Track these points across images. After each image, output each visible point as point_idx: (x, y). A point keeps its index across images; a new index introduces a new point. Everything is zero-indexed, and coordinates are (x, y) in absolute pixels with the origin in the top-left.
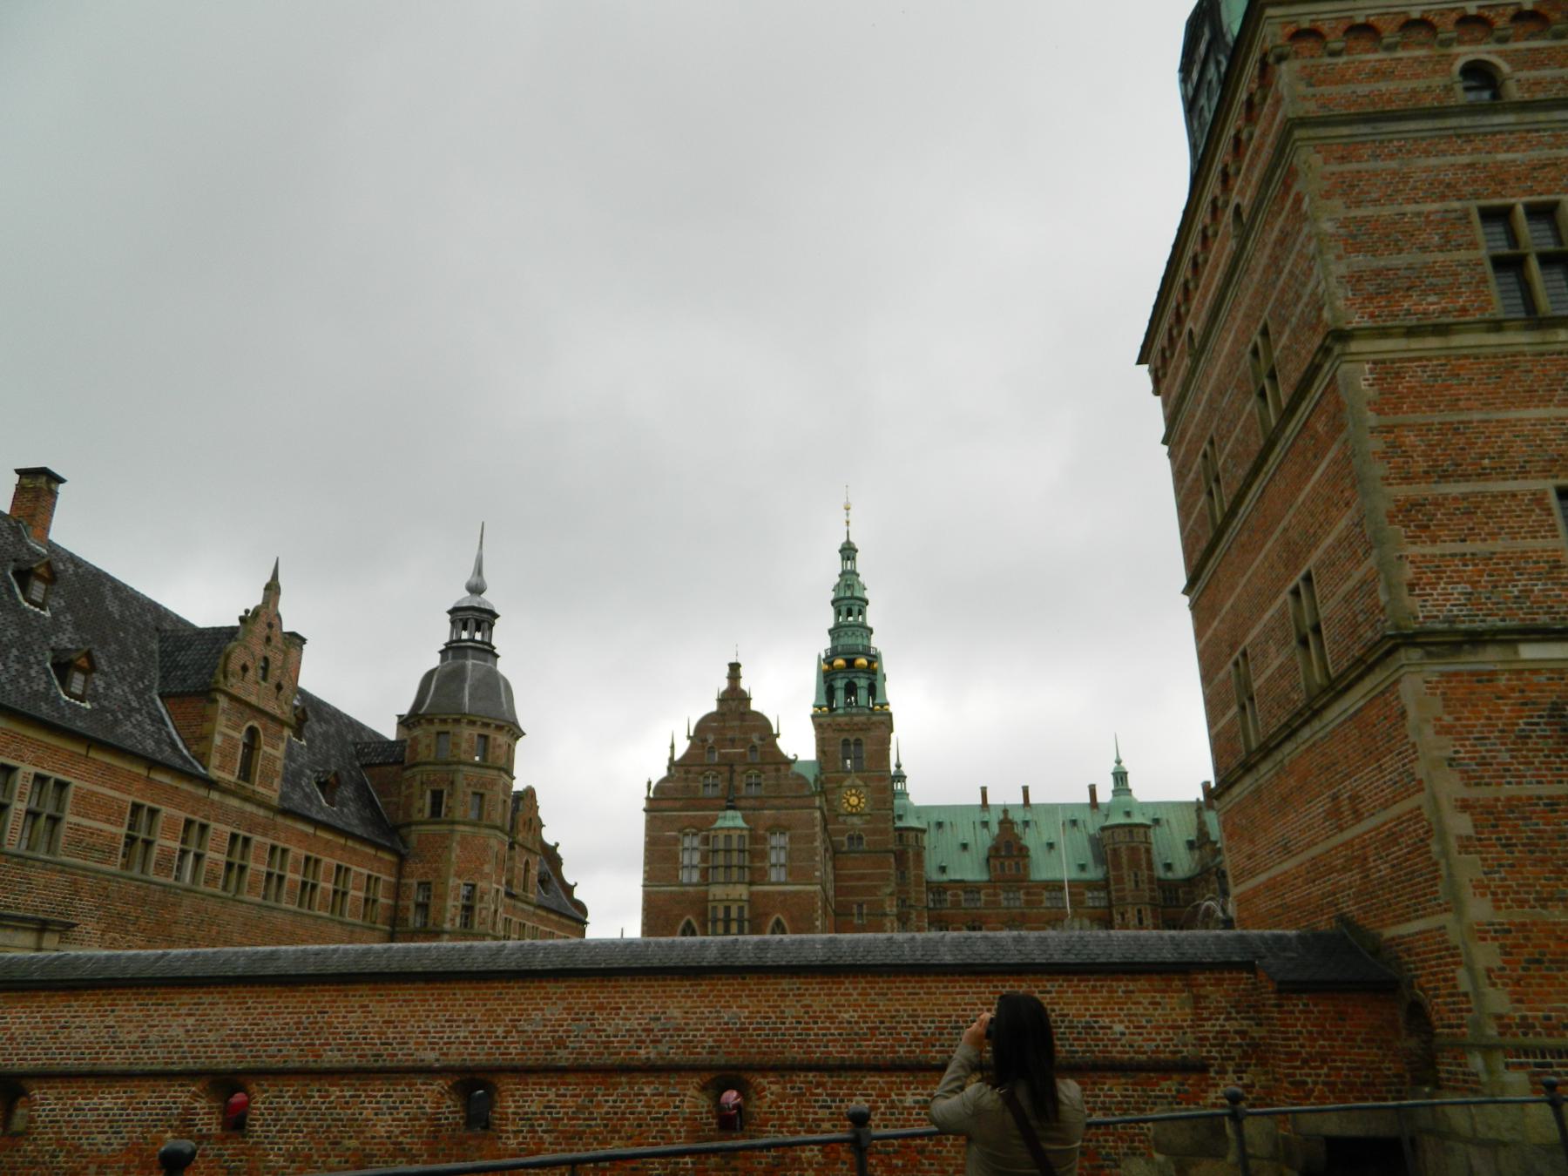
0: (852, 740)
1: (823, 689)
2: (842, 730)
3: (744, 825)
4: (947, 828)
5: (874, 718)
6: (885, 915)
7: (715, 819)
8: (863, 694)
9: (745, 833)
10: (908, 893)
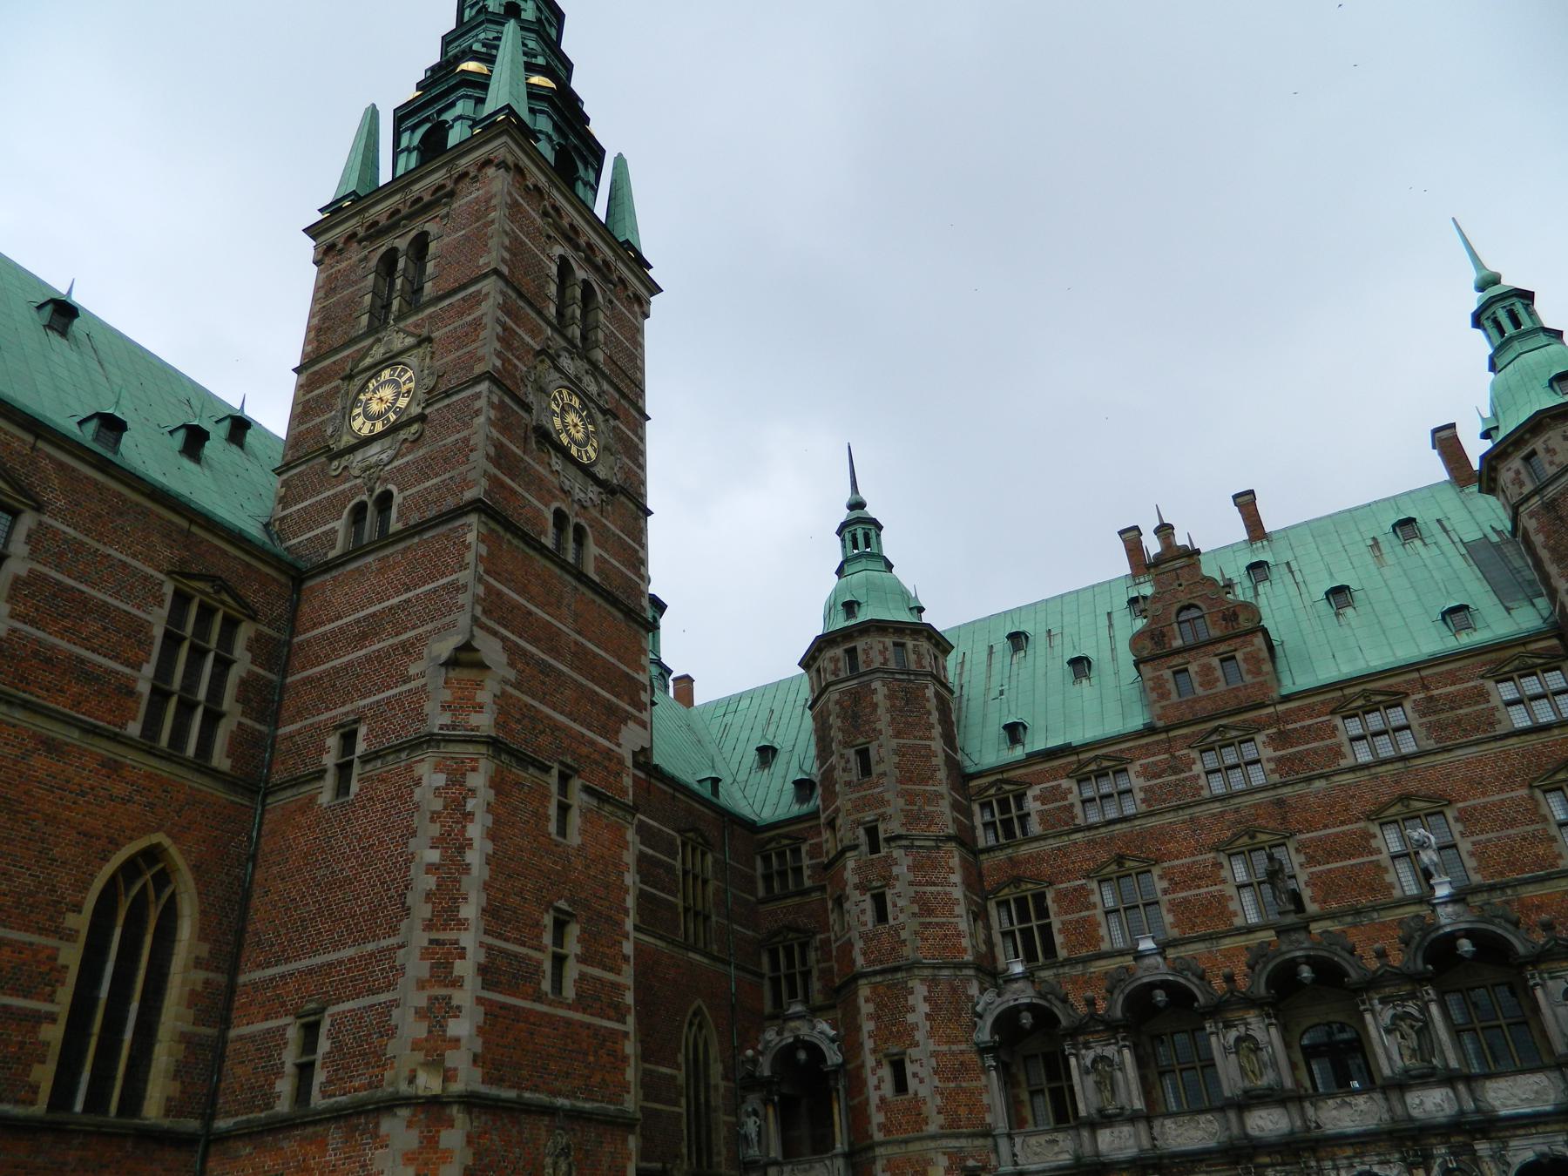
4: (1038, 645)
10: (883, 802)
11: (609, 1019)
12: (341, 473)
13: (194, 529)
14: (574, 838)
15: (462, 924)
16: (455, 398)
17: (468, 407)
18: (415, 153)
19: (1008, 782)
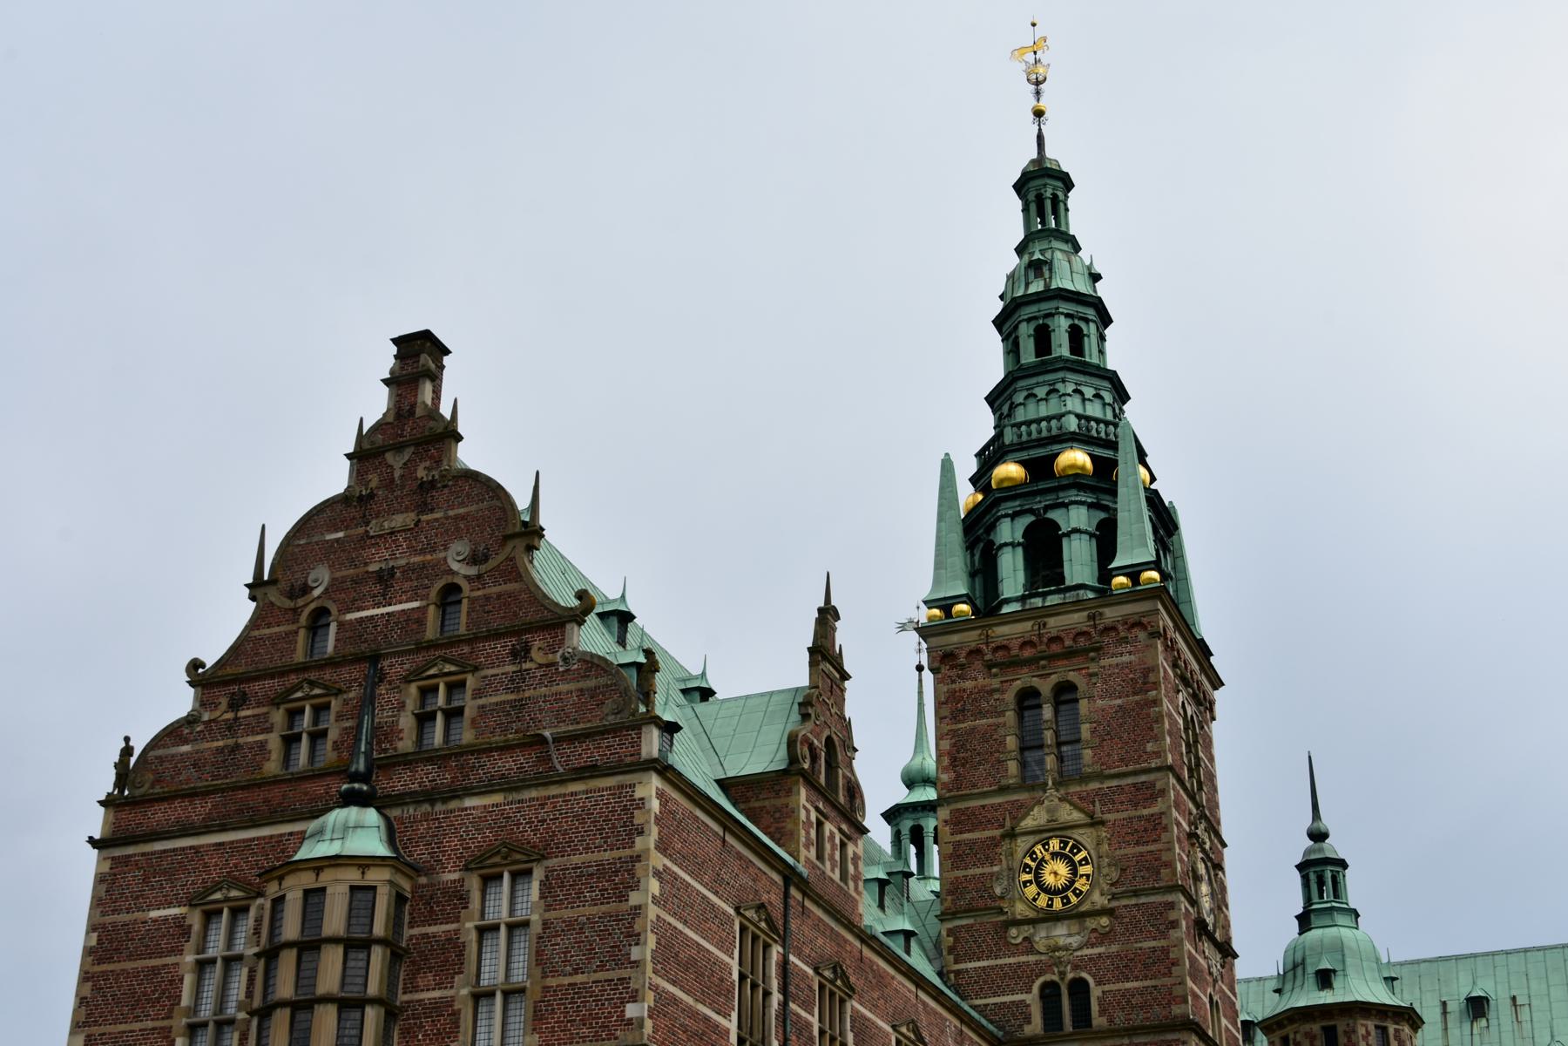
0: (1045, 687)
1: (958, 560)
2: (1016, 664)
3: (382, 850)
4: (1500, 1010)
5: (1111, 614)
7: (302, 837)
8: (1079, 562)
9: (376, 876)
12: (1021, 943)
13: (965, 1029)
16: (1143, 900)
17: (1161, 914)
18: (1020, 551)
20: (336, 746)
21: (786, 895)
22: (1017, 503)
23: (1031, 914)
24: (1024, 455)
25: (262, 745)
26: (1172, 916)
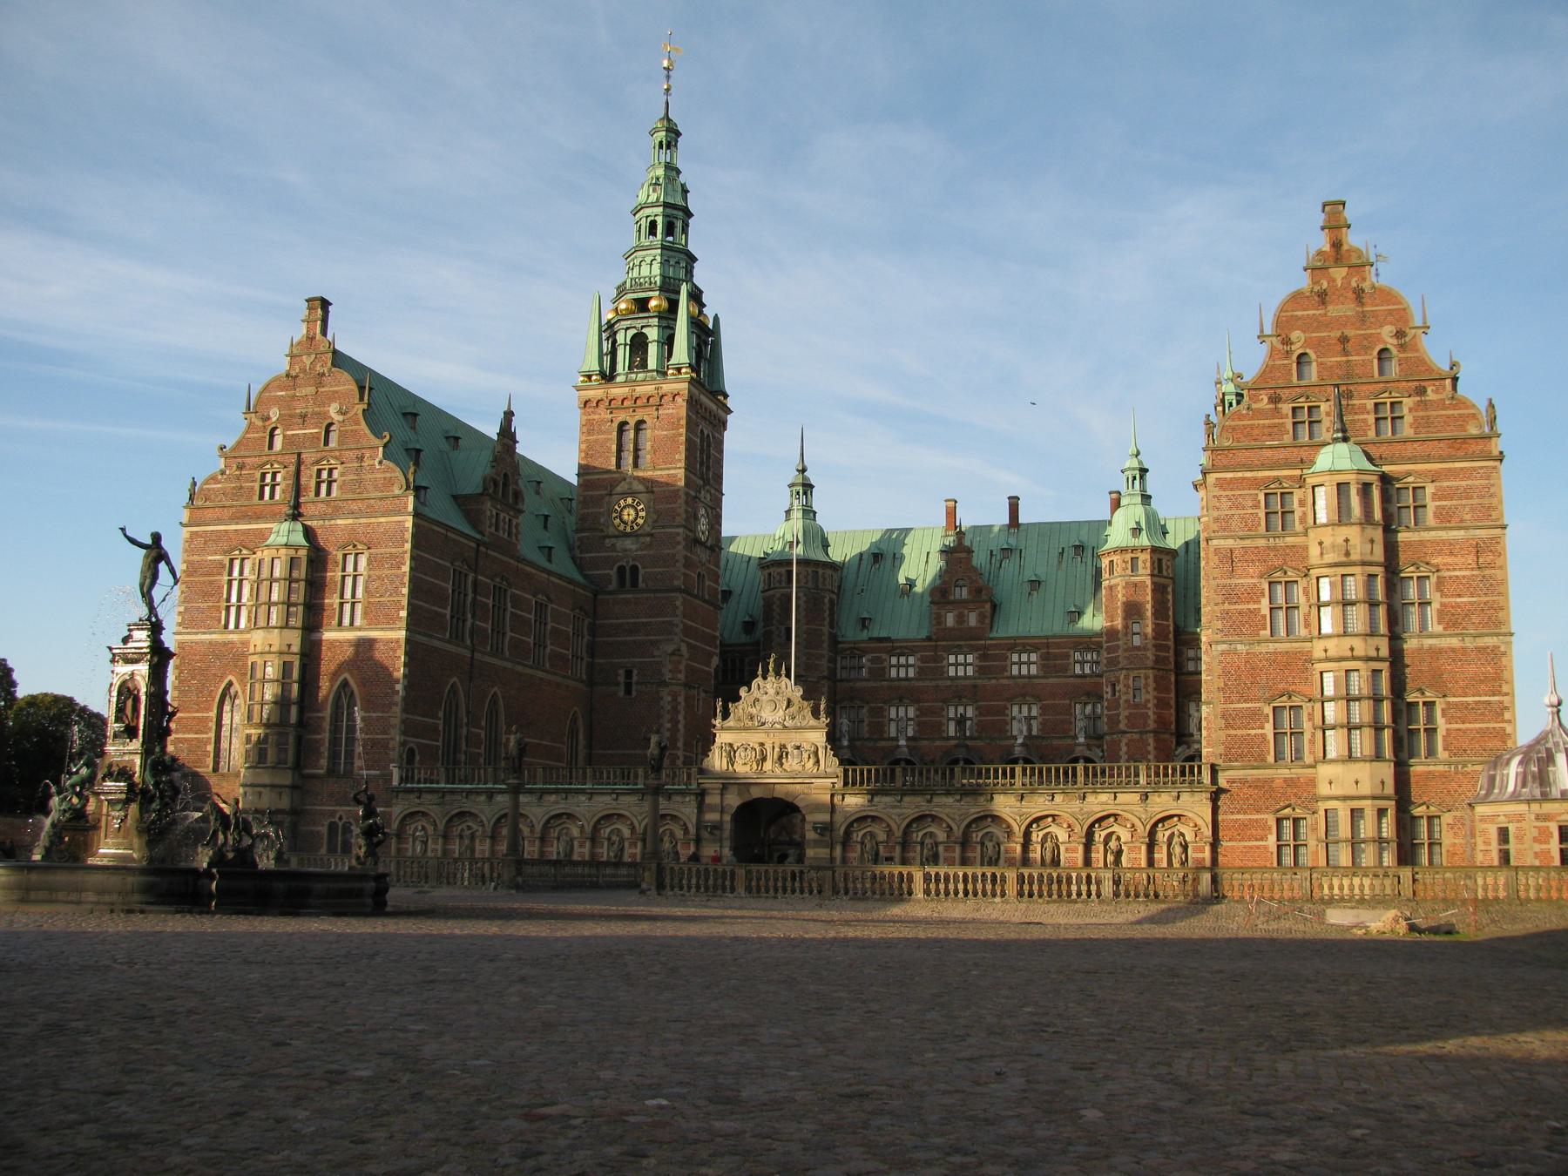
6: (663, 683)
11: (421, 600)
13: (577, 589)
14: (700, 712)
15: (678, 749)
16: (667, 530)
18: (628, 347)
19: (857, 649)
20: (283, 491)
21: (478, 551)
22: (629, 322)
23: (617, 533)
24: (635, 296)
25: (252, 488)
26: (680, 538)
